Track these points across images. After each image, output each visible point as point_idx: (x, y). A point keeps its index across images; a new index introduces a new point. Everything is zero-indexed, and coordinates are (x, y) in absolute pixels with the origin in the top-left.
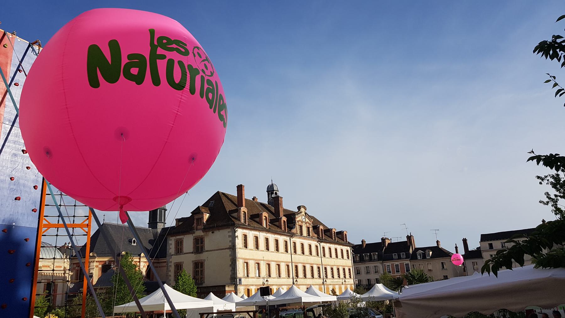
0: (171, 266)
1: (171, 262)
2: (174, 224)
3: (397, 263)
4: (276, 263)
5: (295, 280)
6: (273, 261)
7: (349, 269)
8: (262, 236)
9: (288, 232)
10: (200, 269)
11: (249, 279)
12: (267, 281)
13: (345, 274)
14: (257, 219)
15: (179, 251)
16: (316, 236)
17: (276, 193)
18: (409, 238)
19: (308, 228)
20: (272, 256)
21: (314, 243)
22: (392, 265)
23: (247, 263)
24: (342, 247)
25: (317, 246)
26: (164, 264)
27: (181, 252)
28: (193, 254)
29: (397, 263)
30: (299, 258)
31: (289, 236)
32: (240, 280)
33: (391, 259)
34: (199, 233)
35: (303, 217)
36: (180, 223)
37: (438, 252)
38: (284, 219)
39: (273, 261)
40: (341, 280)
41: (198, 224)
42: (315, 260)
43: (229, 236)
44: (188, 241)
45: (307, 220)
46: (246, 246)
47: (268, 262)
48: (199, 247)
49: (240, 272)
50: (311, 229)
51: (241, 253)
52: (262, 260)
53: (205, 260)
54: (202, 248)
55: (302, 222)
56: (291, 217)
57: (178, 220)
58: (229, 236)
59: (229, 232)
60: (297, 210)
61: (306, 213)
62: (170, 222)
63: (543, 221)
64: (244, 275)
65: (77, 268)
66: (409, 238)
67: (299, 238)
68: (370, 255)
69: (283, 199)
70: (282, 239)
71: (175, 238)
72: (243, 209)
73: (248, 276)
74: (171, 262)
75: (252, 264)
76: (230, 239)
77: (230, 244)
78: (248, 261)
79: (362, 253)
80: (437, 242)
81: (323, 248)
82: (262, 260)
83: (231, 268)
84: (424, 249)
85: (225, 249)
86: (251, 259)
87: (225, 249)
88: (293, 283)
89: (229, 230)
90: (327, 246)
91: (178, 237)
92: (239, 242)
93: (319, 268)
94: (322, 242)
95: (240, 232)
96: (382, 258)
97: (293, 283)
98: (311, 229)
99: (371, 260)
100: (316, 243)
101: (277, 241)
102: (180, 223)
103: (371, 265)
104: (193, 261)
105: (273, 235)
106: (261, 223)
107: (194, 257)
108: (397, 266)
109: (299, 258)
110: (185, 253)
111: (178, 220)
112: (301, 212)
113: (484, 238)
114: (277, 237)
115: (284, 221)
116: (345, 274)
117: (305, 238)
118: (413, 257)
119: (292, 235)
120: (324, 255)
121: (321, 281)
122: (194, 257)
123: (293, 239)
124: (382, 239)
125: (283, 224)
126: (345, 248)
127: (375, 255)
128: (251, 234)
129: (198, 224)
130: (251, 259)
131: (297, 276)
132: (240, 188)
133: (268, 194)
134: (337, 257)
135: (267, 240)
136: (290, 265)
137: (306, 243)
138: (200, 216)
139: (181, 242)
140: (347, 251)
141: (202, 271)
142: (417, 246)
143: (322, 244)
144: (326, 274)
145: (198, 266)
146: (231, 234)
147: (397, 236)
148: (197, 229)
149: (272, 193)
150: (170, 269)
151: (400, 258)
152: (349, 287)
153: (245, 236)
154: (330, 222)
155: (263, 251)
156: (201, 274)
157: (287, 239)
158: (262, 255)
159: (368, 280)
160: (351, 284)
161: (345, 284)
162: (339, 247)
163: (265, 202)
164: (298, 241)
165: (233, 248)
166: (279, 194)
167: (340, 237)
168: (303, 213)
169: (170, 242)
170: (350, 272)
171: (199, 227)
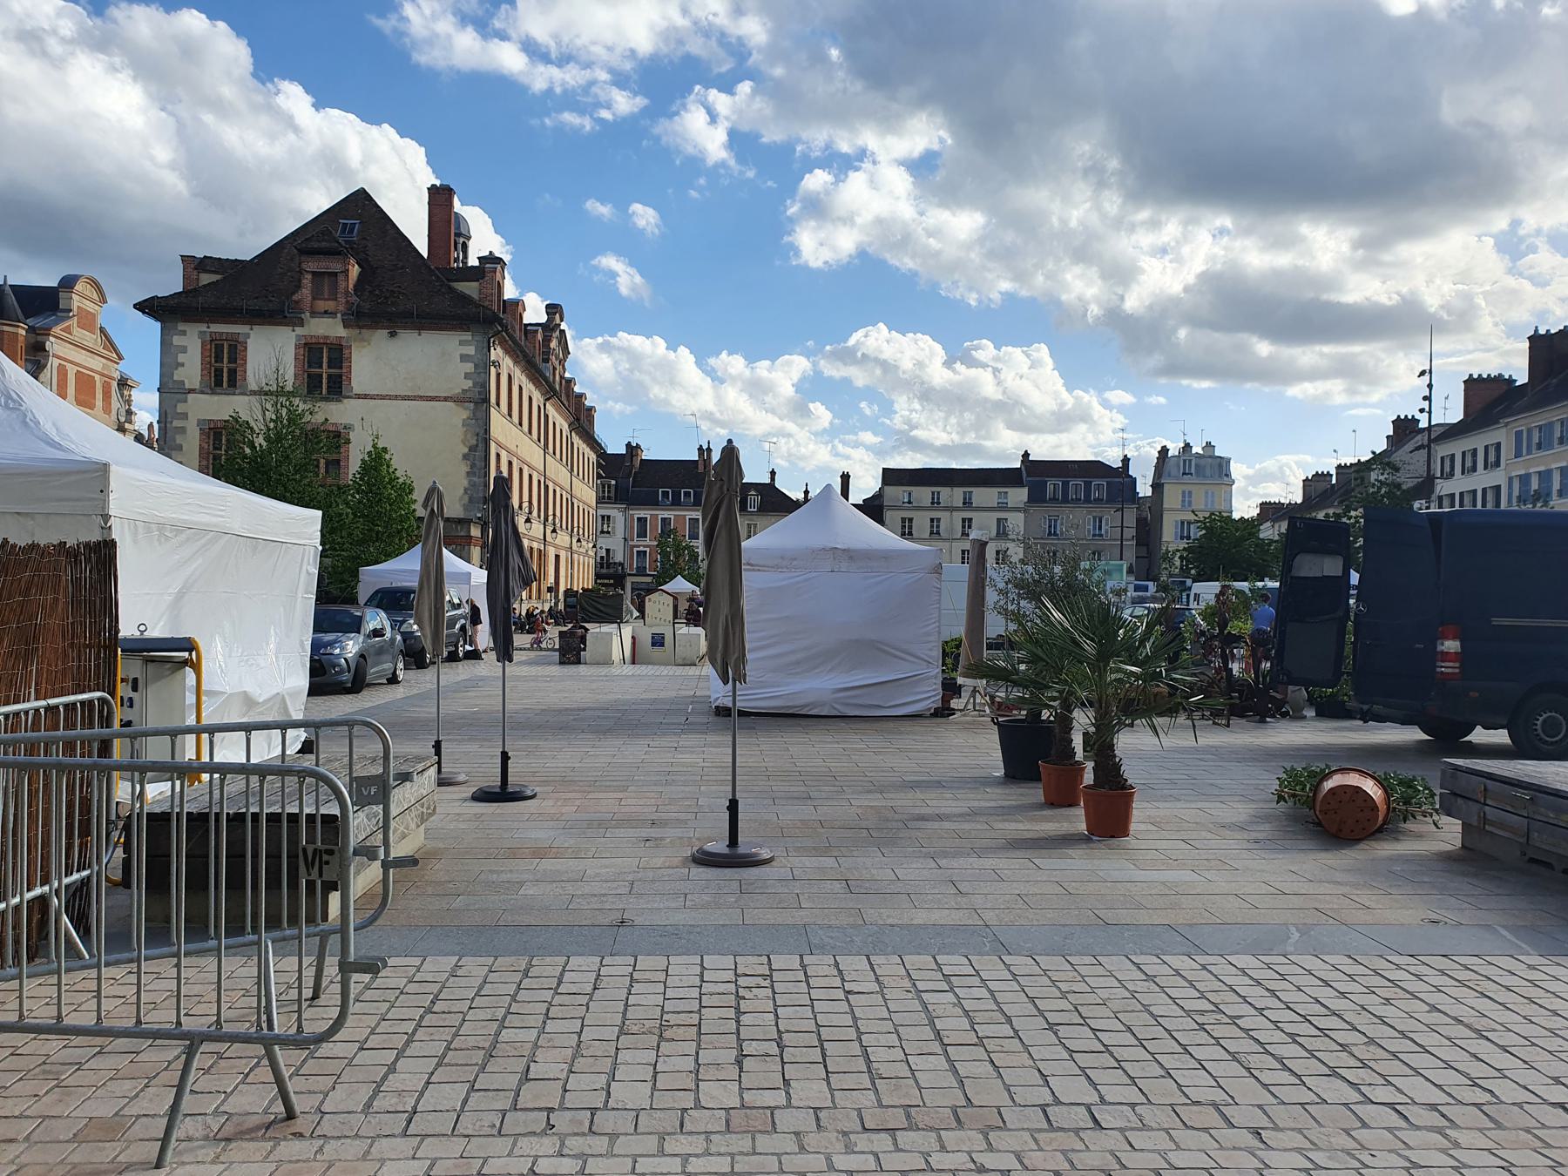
0: (183, 430)
1: (185, 416)
3: (666, 514)
27: (233, 383)
29: (666, 514)
33: (652, 502)
34: (330, 328)
36: (206, 279)
59: (462, 343)
63: (1026, 455)
71: (203, 327)
74: (185, 416)
76: (469, 367)
80: (773, 473)
83: (465, 468)
87: (446, 399)
89: (467, 336)
113: (890, 476)
124: (628, 445)
129: (316, 296)
146: (471, 350)
148: (314, 314)
151: (676, 503)
171: (322, 305)
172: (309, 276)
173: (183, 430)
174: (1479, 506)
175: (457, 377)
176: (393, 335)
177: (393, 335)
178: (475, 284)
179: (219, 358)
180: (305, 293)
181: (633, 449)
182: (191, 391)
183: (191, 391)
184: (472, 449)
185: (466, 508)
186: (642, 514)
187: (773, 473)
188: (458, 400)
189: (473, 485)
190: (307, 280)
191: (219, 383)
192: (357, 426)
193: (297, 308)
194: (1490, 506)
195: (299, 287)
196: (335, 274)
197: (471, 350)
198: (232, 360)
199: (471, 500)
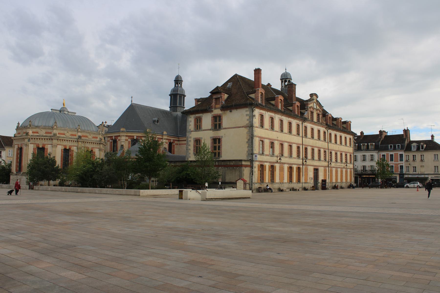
0: (190, 141)
2: (194, 105)
3: (391, 153)
5: (304, 161)
6: (286, 142)
7: (351, 155)
8: (277, 117)
9: (300, 117)
10: (217, 145)
11: (264, 157)
12: (280, 159)
13: (346, 159)
14: (273, 102)
15: (198, 127)
16: (325, 123)
17: (289, 81)
18: (406, 132)
19: (318, 115)
20: (285, 137)
21: (322, 129)
22: (388, 154)
23: (263, 141)
24: (346, 135)
25: (325, 132)
26: (185, 142)
27: (200, 129)
28: (211, 131)
29: (391, 153)
30: (308, 142)
31: (301, 120)
32: (256, 156)
33: (386, 149)
34: (217, 112)
35: (315, 104)
36: (199, 103)
37: (430, 145)
38: (298, 104)
39: (286, 142)
40: (343, 165)
41: (216, 104)
42: (322, 144)
43: (247, 115)
44: (207, 120)
46: (262, 126)
48: (217, 124)
49: (256, 150)
50: (321, 116)
51: (258, 132)
53: (222, 137)
54: (220, 125)
55: (314, 109)
56: (304, 104)
57: (197, 100)
58: (247, 115)
59: (246, 111)
60: (310, 98)
61: (317, 101)
62: (189, 103)
64: (259, 152)
65: (110, 141)
66: (406, 132)
67: (310, 123)
68: (368, 146)
69: (296, 87)
70: (295, 122)
72: (261, 90)
73: (263, 153)
74: (191, 137)
75: (267, 143)
76: (248, 117)
77: (248, 122)
78: (264, 140)
79: (363, 142)
80: (432, 136)
81: (330, 134)
82: (276, 140)
83: (247, 145)
84: (418, 142)
86: (267, 138)
87: (242, 127)
88: (303, 164)
89: (247, 109)
90: (333, 133)
91: (197, 115)
92: (256, 121)
93: (325, 152)
94: (330, 129)
95: (257, 112)
96: (377, 148)
97: (303, 164)
98: (321, 116)
99: (368, 149)
100: (324, 129)
101: (290, 124)
102: (199, 103)
103: (368, 154)
104: (211, 138)
105: (287, 118)
106: (276, 106)
107: (212, 134)
108: (392, 156)
109: (308, 142)
110: (204, 130)
111: (197, 100)
112: (313, 100)
114: (290, 119)
115: (298, 106)
116: (346, 159)
117: (314, 123)
118: (408, 148)
119: (305, 120)
120: (331, 141)
121: (326, 164)
122: (212, 134)
123: (305, 124)
124: (380, 132)
125: (296, 108)
126: (348, 137)
127: (372, 145)
128: (267, 115)
129: (216, 104)
130: (267, 138)
131: (306, 157)
132: (258, 72)
133: (282, 82)
134: (341, 143)
135: (282, 121)
136: (301, 146)
137: (316, 128)
138: (219, 96)
139: (200, 120)
140: (350, 139)
141: (219, 147)
142: (412, 139)
143: (330, 131)
144: (331, 158)
145: (217, 141)
147: (394, 129)
148: (215, 108)
149: (286, 81)
150: (190, 143)
151: (395, 149)
152: (349, 170)
153: (262, 116)
154: (334, 113)
155: (277, 132)
156: (219, 149)
157: (300, 123)
158: (275, 135)
159: (363, 166)
160: (351, 169)
161: (346, 168)
162: (343, 135)
163: (279, 88)
164: (309, 126)
165: (251, 126)
166: (293, 81)
167: (344, 127)
168: (315, 101)
169: (190, 119)
170: (351, 158)
171: (218, 106)
172: (214, 99)
173: (190, 141)
175: (245, 121)
176: (231, 111)
177: (231, 111)
178: (254, 94)
179: (197, 123)
180: (213, 104)
181: (362, 133)
182: (192, 131)
183: (192, 131)
184: (249, 140)
185: (247, 156)
186: (383, 153)
187: (432, 136)
188: (245, 127)
189: (249, 150)
190: (214, 100)
191: (197, 129)
192: (224, 136)
193: (211, 107)
195: (211, 104)
196: (219, 98)
197: (248, 113)
198: (200, 122)
199: (248, 154)
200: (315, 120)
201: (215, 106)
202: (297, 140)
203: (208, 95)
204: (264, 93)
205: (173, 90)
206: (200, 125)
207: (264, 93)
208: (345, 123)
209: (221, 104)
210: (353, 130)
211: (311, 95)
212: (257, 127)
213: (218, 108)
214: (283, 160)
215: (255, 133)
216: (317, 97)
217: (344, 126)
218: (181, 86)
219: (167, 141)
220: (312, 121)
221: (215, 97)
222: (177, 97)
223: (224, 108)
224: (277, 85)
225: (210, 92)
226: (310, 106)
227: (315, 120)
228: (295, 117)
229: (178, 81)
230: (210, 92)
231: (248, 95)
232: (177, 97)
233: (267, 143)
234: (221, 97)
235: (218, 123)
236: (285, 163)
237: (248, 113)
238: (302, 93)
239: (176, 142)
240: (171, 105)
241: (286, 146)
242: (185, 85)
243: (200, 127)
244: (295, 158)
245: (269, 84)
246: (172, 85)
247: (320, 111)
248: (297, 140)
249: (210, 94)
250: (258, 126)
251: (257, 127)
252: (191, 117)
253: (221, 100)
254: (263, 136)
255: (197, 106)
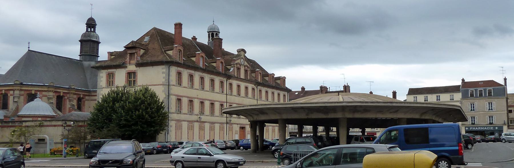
4: (210, 102)
19: (246, 71)
21: (250, 86)
25: (253, 89)
34: (132, 68)
43: (163, 73)
45: (246, 64)
47: (201, 101)
52: (196, 98)
55: (240, 65)
59: (162, 69)
60: (236, 53)
61: (245, 56)
71: (106, 71)
75: (185, 102)
82: (196, 98)
85: (158, 85)
87: (158, 85)
89: (164, 66)
91: (110, 71)
100: (253, 86)
102: (112, 57)
105: (209, 75)
111: (111, 54)
119: (229, 77)
123: (231, 81)
124: (321, 87)
126: (282, 93)
129: (130, 59)
132: (179, 26)
137: (243, 85)
143: (259, 87)
155: (198, 89)
164: (235, 83)
166: (221, 36)
168: (242, 56)
169: (101, 75)
171: (132, 62)
174: (282, 101)
179: (110, 79)
182: (104, 88)
183: (104, 88)
190: (128, 56)
191: (110, 85)
194: (282, 101)
196: (134, 53)
200: (242, 76)
201: (130, 62)
202: (222, 98)
203: (123, 49)
204: (182, 50)
205: (84, 35)
206: (112, 81)
207: (182, 50)
208: (279, 78)
209: (136, 60)
210: (288, 85)
211: (239, 51)
212: (174, 85)
213: (133, 64)
214: (203, 118)
215: (172, 92)
216: (245, 52)
217: (278, 81)
218: (94, 31)
219: (75, 96)
220: (238, 79)
221: (129, 52)
222: (89, 44)
223: (139, 65)
224: (204, 39)
225: (125, 47)
226: (236, 62)
227: (242, 76)
228: (218, 74)
229: (91, 24)
230: (125, 47)
231: (165, 51)
232: (89, 44)
233: (185, 102)
234: (137, 53)
235: (132, 79)
236: (205, 122)
237: (164, 70)
238: (229, 47)
239: (87, 97)
240: (81, 53)
241: (207, 104)
242: (100, 32)
243: (112, 83)
244: (217, 116)
245: (194, 38)
246: (83, 29)
247: (248, 67)
248: (222, 98)
249: (124, 49)
250: (175, 84)
251: (174, 85)
252: (102, 73)
253: (136, 56)
254: (181, 94)
255: (111, 60)
